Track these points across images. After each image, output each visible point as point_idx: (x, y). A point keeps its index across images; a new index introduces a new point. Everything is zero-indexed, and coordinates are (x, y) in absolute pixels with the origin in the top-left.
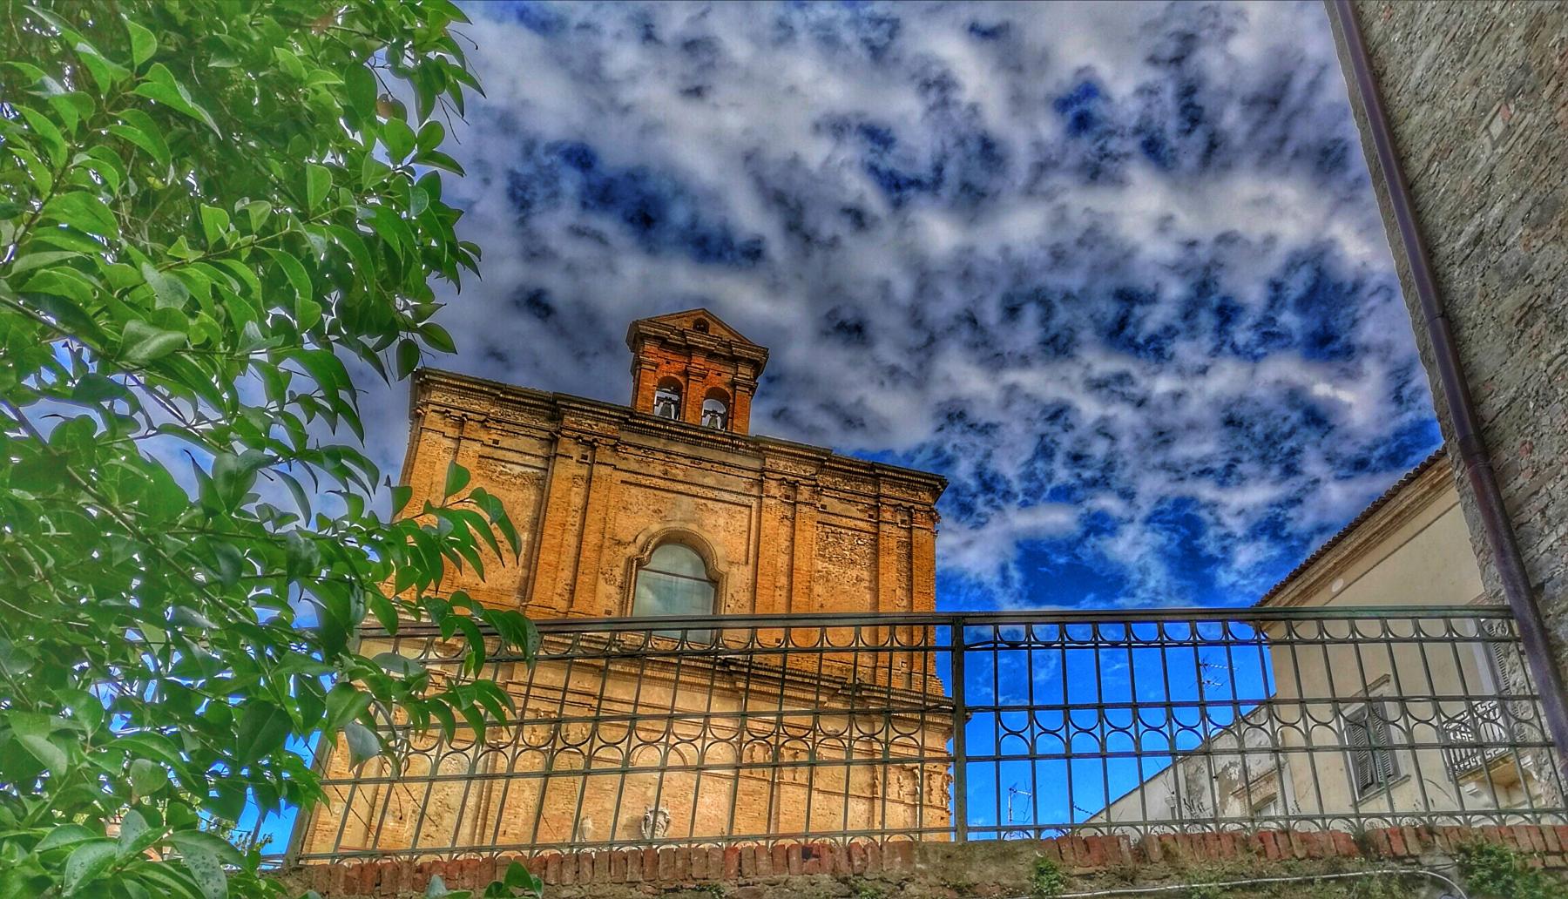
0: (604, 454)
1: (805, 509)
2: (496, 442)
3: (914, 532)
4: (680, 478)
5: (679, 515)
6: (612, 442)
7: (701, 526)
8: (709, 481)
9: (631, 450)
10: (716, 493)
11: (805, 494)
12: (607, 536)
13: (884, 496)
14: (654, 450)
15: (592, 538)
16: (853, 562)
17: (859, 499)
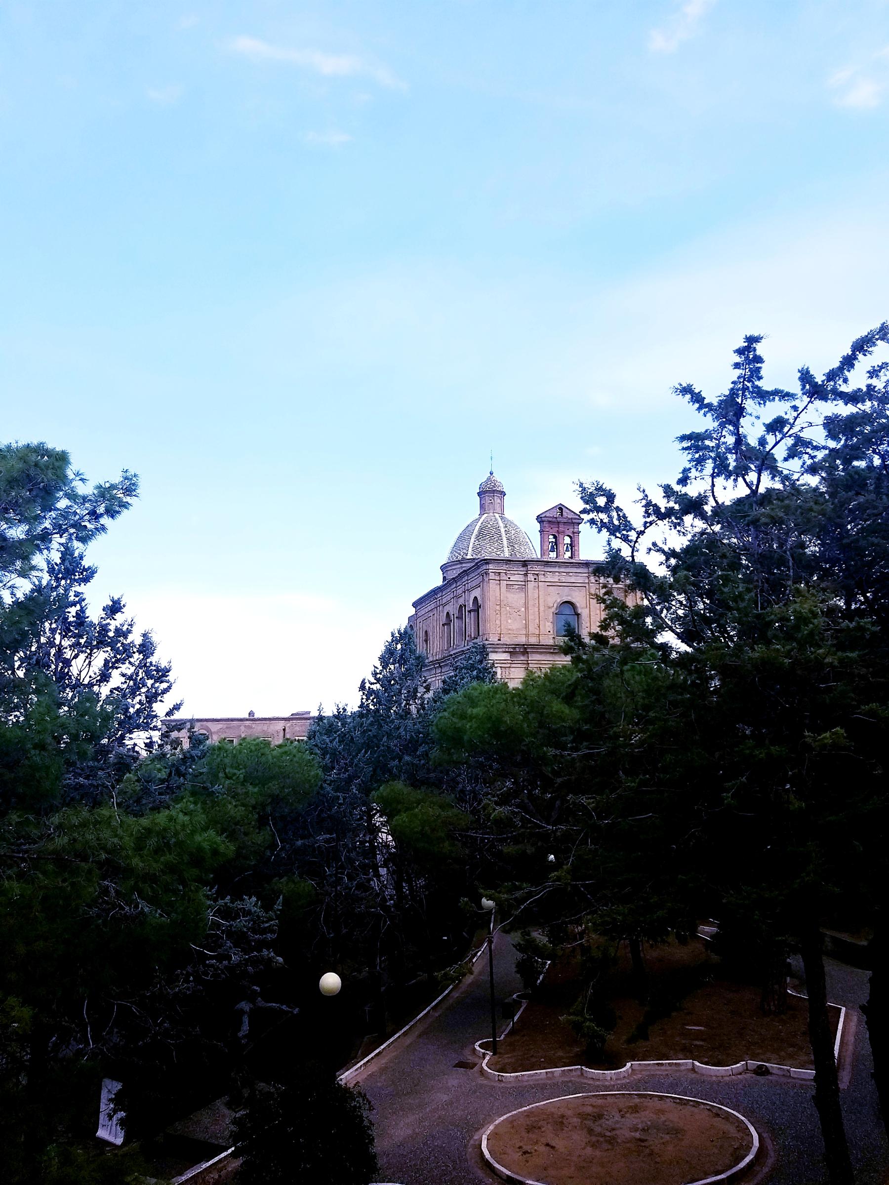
0: (541, 578)
2: (509, 578)
15: (542, 609)
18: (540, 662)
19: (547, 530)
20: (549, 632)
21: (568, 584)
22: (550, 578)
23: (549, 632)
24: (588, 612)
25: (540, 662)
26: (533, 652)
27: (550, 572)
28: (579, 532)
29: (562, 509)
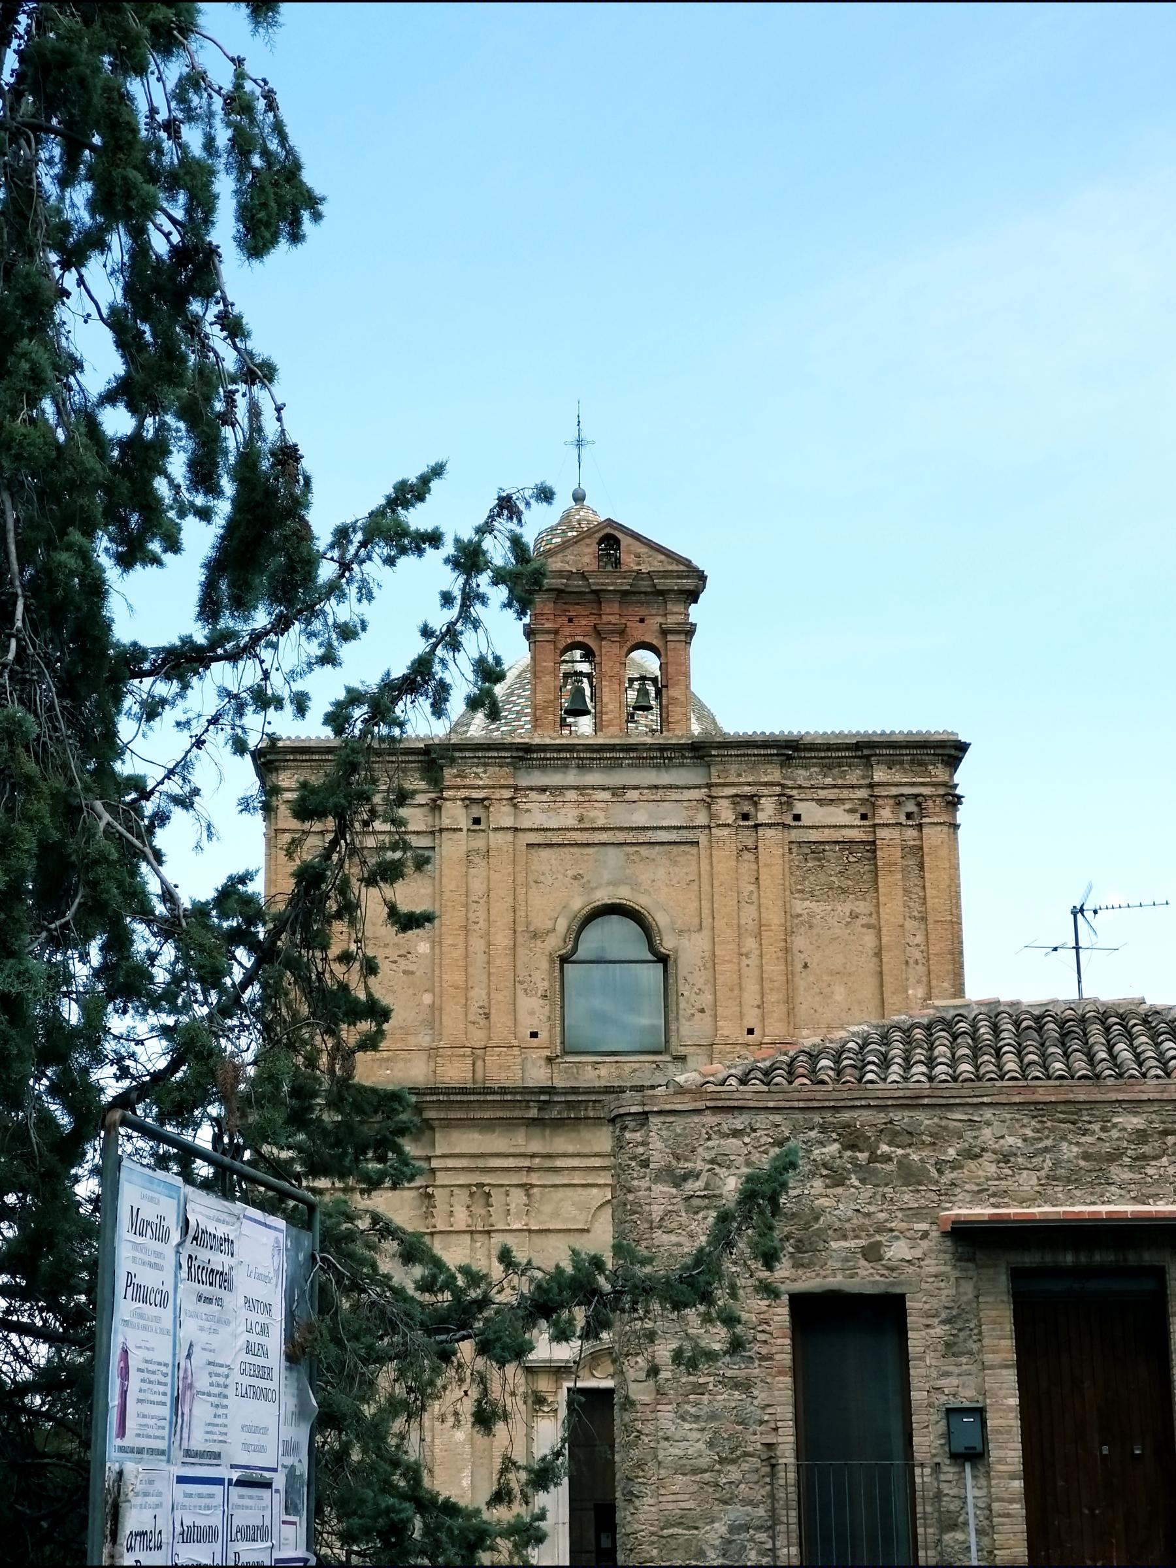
0: (502, 816)
1: (770, 833)
3: (926, 830)
4: (600, 822)
5: (606, 876)
6: (508, 794)
7: (635, 886)
8: (640, 818)
9: (534, 795)
10: (650, 833)
11: (767, 811)
12: (519, 929)
13: (879, 785)
14: (562, 789)
16: (844, 891)
17: (845, 794)
18: (481, 1163)
19: (548, 625)
20: (534, 1035)
21: (620, 837)
22: (537, 814)
23: (534, 1035)
24: (707, 947)
25: (481, 1163)
26: (449, 1124)
27: (543, 790)
28: (689, 631)
29: (617, 541)
